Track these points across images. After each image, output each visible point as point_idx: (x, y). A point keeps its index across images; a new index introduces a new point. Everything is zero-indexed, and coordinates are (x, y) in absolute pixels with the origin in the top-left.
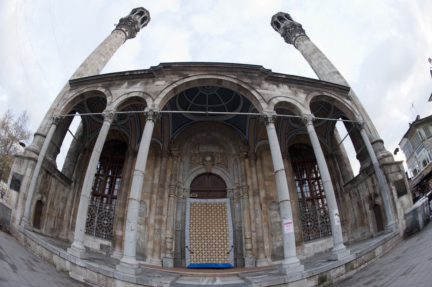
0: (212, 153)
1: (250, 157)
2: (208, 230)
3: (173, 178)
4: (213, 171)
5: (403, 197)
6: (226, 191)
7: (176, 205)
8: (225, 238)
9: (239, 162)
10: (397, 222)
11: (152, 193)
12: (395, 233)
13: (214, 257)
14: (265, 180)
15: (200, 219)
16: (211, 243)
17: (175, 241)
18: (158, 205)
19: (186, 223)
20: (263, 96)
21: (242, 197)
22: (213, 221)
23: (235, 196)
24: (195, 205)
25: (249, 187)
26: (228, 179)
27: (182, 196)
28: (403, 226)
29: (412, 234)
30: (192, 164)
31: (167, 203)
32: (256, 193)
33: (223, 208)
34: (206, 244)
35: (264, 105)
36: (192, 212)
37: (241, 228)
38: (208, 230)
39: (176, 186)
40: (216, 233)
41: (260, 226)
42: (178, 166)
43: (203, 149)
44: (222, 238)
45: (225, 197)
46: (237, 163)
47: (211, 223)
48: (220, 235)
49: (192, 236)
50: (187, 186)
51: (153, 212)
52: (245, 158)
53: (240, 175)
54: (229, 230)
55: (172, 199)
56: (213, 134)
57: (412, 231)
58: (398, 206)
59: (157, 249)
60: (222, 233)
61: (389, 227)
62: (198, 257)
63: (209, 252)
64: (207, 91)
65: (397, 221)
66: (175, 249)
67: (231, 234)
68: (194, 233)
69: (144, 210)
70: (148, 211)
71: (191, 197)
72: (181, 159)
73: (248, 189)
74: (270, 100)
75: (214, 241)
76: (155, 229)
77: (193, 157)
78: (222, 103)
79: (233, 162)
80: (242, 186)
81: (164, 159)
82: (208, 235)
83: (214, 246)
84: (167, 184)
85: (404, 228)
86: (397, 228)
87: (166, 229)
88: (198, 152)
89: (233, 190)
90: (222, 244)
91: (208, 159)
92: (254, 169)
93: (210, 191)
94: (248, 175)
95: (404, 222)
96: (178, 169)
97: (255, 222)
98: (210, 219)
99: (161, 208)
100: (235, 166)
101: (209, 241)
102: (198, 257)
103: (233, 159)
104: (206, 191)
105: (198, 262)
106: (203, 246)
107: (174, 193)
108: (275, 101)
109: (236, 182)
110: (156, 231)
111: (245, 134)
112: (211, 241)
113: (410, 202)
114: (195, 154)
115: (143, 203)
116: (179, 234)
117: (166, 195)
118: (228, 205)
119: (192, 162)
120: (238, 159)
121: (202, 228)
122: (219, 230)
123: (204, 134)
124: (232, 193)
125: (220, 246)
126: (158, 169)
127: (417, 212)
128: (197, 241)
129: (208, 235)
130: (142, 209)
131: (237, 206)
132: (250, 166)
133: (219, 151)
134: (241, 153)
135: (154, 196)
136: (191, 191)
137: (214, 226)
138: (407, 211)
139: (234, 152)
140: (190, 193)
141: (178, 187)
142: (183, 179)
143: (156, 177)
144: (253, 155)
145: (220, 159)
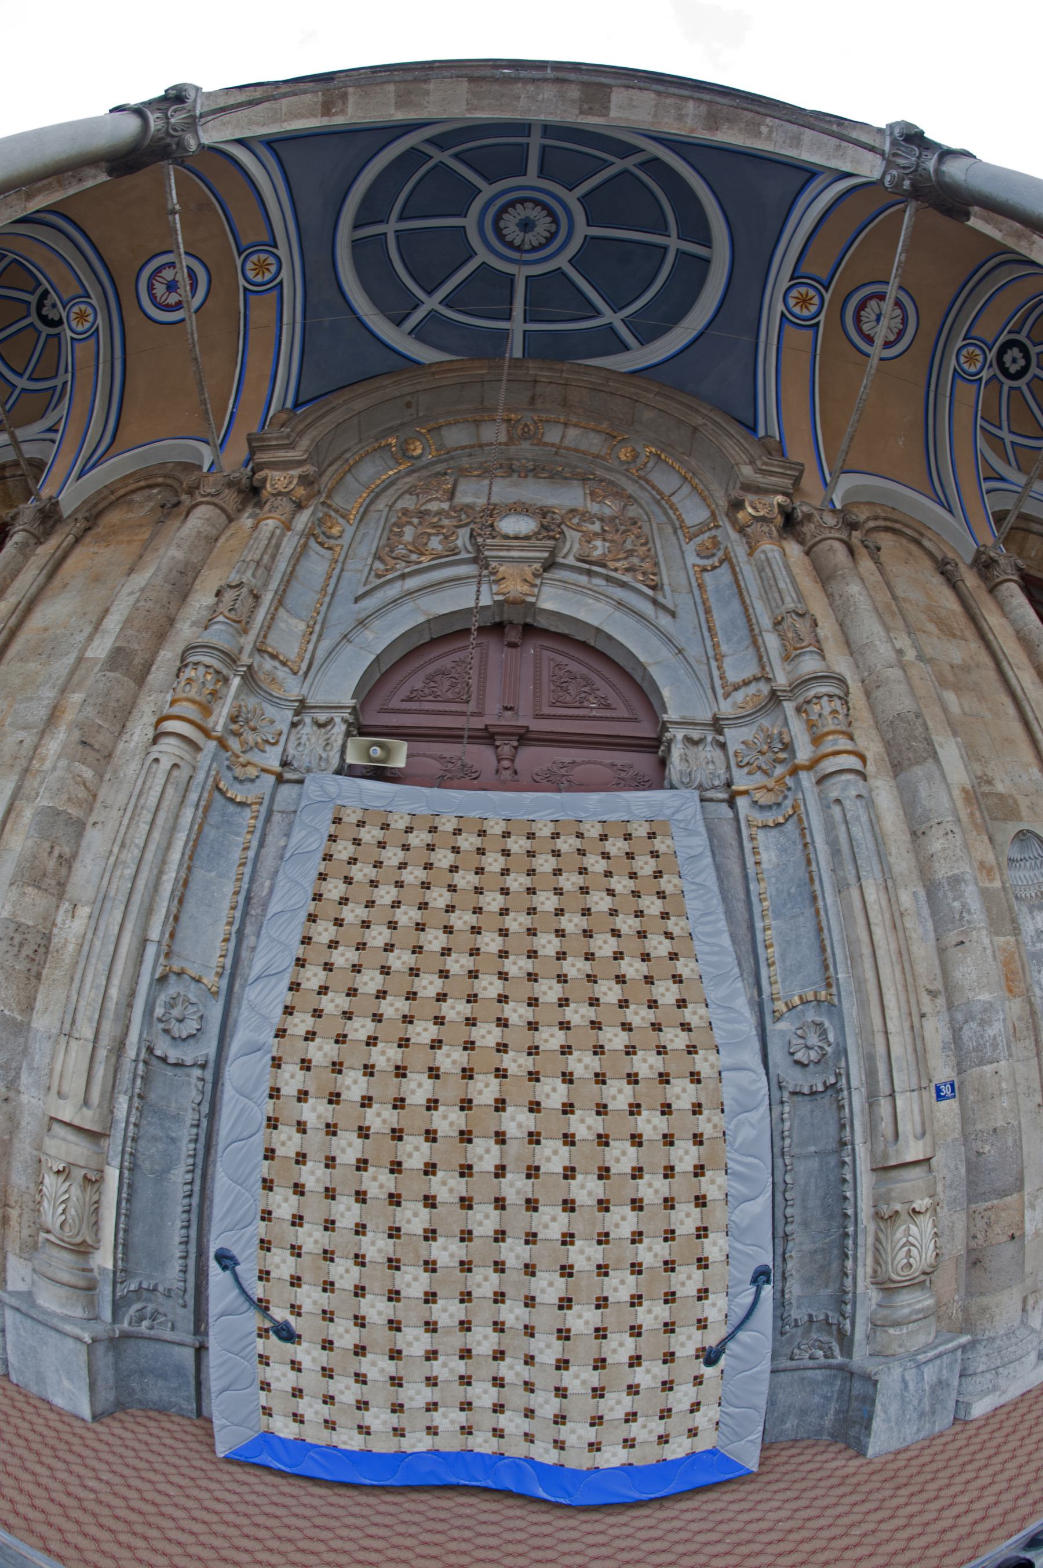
1: (809, 529)
3: (224, 607)
4: (552, 600)
8: (682, 1187)
14: (942, 682)
16: (514, 1252)
17: (131, 1169)
21: (810, 767)
23: (738, 774)
26: (666, 653)
27: (272, 759)
32: (906, 752)
33: (645, 866)
34: (446, 1252)
36: (334, 889)
40: (585, 1125)
44: (652, 1188)
46: (727, 559)
48: (622, 1157)
49: (287, 1142)
50: (339, 686)
53: (765, 621)
54: (728, 1094)
56: (553, 435)
60: (651, 1124)
67: (753, 1127)
68: (315, 1112)
71: (345, 770)
75: (552, 1223)
79: (692, 559)
81: (200, 519)
82: (484, 1155)
84: (168, 655)
89: (717, 725)
93: (524, 737)
96: (282, 566)
101: (484, 1220)
103: (690, 549)
104: (488, 736)
107: (206, 710)
112: (518, 1220)
114: (422, 514)
118: (689, 843)
119: (401, 550)
120: (734, 535)
121: (418, 1059)
123: (493, 433)
125: (621, 1286)
129: (484, 1155)
131: (769, 851)
133: (594, 508)
135: (53, 746)
141: (250, 677)
143: (113, 623)
145: (598, 543)
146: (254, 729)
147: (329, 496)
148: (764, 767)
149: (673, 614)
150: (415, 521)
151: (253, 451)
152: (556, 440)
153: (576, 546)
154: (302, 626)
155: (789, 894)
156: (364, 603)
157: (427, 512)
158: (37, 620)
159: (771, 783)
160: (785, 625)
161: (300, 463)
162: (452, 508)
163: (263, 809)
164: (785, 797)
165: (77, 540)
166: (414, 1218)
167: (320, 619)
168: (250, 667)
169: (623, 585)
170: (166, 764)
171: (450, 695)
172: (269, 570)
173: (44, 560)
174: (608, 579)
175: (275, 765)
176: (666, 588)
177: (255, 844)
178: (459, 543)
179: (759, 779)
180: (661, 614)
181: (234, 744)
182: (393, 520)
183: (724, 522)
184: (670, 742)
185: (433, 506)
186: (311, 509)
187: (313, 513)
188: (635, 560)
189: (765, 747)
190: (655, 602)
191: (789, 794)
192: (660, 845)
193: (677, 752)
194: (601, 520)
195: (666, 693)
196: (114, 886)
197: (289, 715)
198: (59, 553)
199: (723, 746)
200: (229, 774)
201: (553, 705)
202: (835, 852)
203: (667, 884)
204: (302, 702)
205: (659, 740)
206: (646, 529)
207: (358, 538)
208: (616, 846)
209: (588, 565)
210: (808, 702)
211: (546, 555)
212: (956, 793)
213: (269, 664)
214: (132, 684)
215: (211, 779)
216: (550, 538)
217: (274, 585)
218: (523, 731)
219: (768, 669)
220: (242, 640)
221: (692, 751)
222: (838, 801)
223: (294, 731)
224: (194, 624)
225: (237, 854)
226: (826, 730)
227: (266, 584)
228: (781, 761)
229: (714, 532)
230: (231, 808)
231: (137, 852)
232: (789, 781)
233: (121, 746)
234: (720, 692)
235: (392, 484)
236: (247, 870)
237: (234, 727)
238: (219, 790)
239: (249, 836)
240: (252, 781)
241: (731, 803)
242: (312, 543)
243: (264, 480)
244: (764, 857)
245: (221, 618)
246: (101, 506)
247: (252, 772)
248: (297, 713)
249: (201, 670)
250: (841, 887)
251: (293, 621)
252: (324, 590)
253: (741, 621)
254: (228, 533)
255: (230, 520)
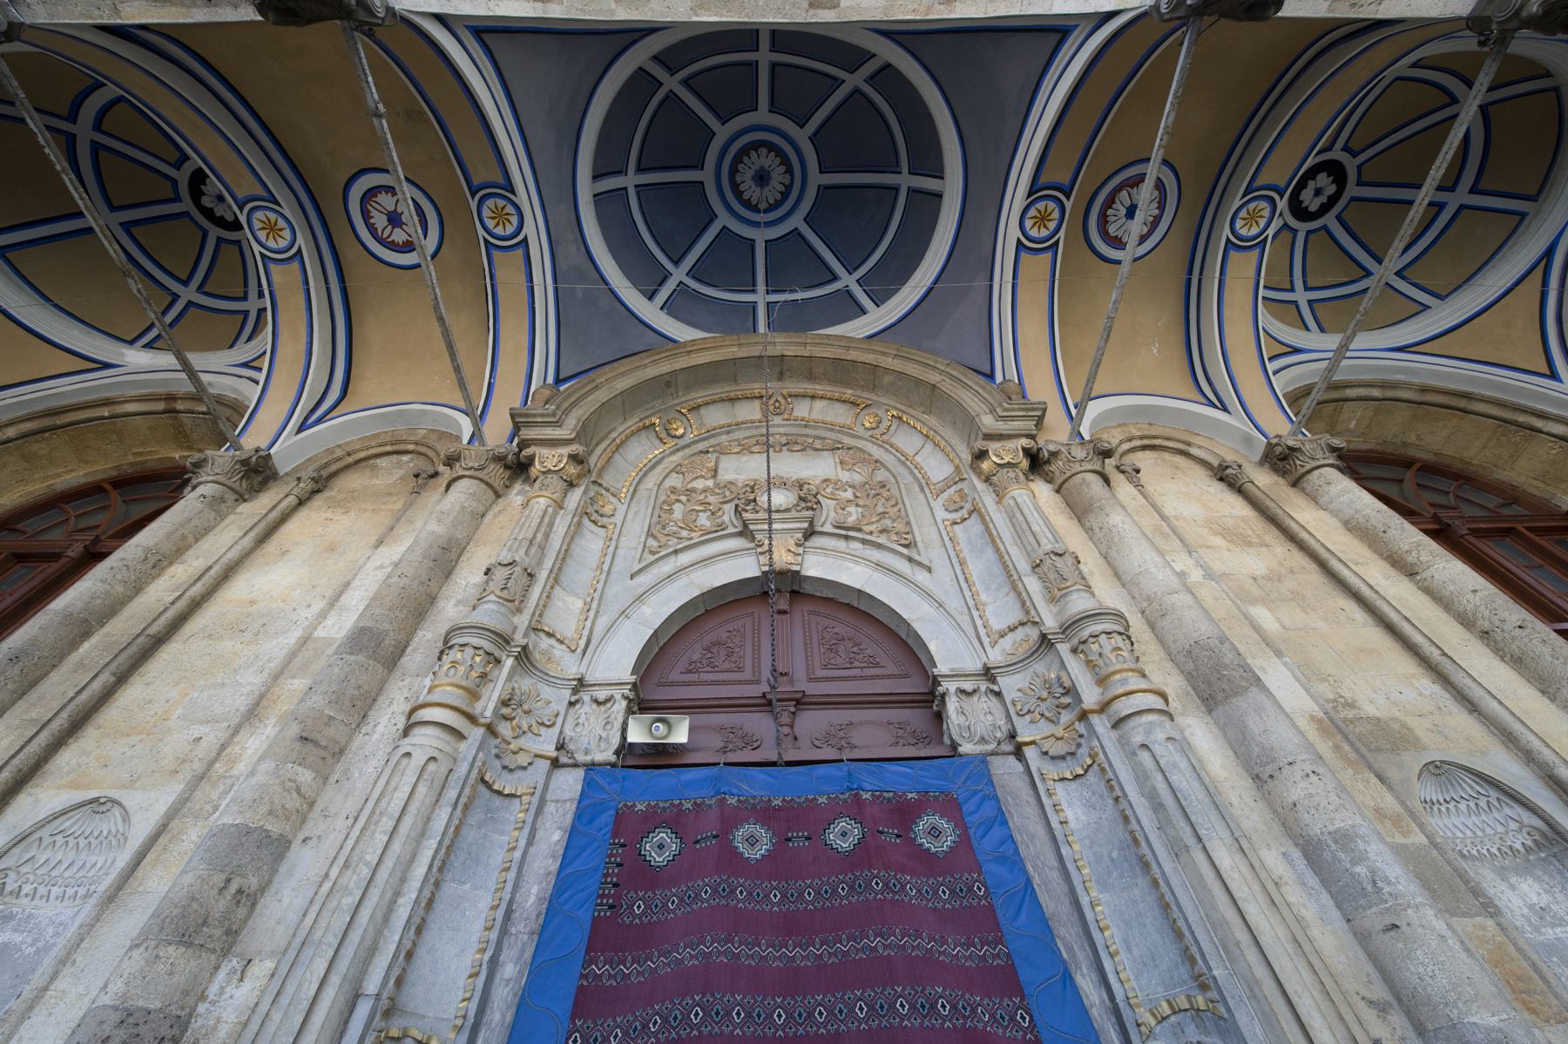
4: (816, 566)
11: (253, 713)
21: (1104, 707)
26: (927, 609)
50: (617, 661)
53: (1023, 565)
56: (802, 409)
77: (678, 508)
79: (941, 514)
80: (1068, 628)
84: (428, 636)
89: (988, 673)
93: (801, 702)
96: (556, 542)
103: (938, 505)
107: (474, 695)
109: (997, 624)
119: (672, 528)
133: (845, 476)
145: (852, 509)
146: (527, 712)
147: (600, 475)
148: (1047, 714)
149: (929, 570)
150: (683, 498)
151: (517, 428)
152: (805, 414)
153: (832, 514)
154: (580, 604)
155: (1112, 859)
156: (639, 579)
157: (693, 490)
158: (239, 589)
159: (1059, 732)
160: (1044, 568)
161: (568, 442)
162: (717, 485)
163: (535, 800)
164: (1079, 745)
165: (301, 503)
167: (597, 596)
168: (525, 648)
169: (879, 546)
170: (419, 758)
171: (726, 666)
172: (542, 548)
173: (250, 522)
174: (864, 542)
176: (919, 544)
177: (523, 842)
178: (726, 518)
179: (1045, 728)
180: (917, 570)
181: (505, 729)
182: (663, 498)
184: (943, 696)
185: (699, 484)
186: (582, 488)
187: (585, 492)
188: (887, 523)
189: (1045, 694)
190: (910, 559)
191: (1082, 741)
193: (952, 705)
194: (852, 487)
195: (932, 647)
196: (323, 924)
197: (566, 694)
198: (274, 514)
199: (998, 694)
200: (497, 763)
201: (825, 667)
202: (1158, 807)
204: (580, 680)
205: (932, 693)
206: (895, 492)
207: (630, 516)
209: (845, 532)
210: (1084, 642)
211: (806, 525)
213: (545, 642)
214: (380, 669)
215: (475, 771)
216: (808, 509)
217: (548, 564)
218: (799, 696)
219: (1033, 613)
220: (515, 620)
221: (968, 703)
222: (1144, 746)
223: (572, 711)
224: (459, 602)
225: (499, 857)
226: (1111, 669)
227: (540, 563)
228: (1066, 707)
229: (959, 486)
230: (498, 801)
231: (366, 872)
232: (1081, 727)
233: (358, 740)
234: (986, 640)
235: (659, 462)
236: (512, 875)
237: (504, 711)
238: (483, 781)
239: (516, 833)
240: (524, 768)
241: (1018, 752)
242: (586, 521)
243: (531, 459)
244: (1069, 814)
245: (492, 597)
246: (334, 468)
247: (523, 759)
248: (575, 691)
249: (469, 651)
250: (1178, 851)
251: (570, 599)
252: (600, 567)
253: (997, 570)
254: (496, 509)
255: (498, 495)
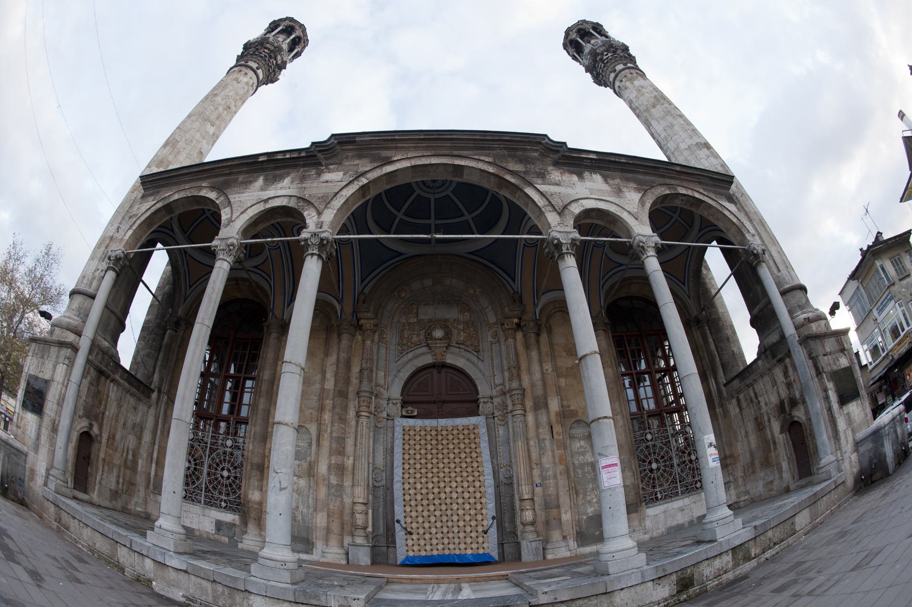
0: (446, 320)
1: (525, 328)
2: (442, 485)
5: (850, 405)
6: (476, 401)
7: (372, 434)
9: (502, 340)
10: (839, 458)
11: (321, 409)
12: (835, 482)
13: (456, 540)
15: (423, 461)
16: (449, 512)
17: (373, 510)
18: (335, 435)
19: (395, 471)
20: (549, 198)
21: (511, 412)
22: (452, 465)
24: (412, 433)
25: (524, 390)
26: (480, 375)
28: (851, 466)
29: (873, 482)
30: (404, 346)
31: (353, 430)
32: (541, 404)
33: (472, 436)
35: (552, 218)
36: (407, 447)
37: (511, 477)
38: (442, 485)
39: (372, 393)
40: (460, 490)
41: (550, 473)
42: (375, 351)
43: (427, 313)
44: (472, 501)
45: (475, 413)
46: (499, 341)
47: (446, 470)
48: (466, 495)
49: (407, 497)
50: (396, 391)
51: (325, 451)
52: (516, 330)
53: (506, 367)
54: (486, 484)
55: (363, 420)
56: (447, 282)
57: (871, 475)
58: (842, 424)
59: (335, 526)
60: (471, 489)
61: (824, 470)
62: (422, 542)
63: (445, 530)
64: (432, 191)
65: (839, 455)
66: (373, 526)
67: (490, 491)
68: (412, 492)
69: (306, 445)
70: (314, 447)
71: (403, 416)
72: (380, 335)
73: (524, 395)
74: (565, 207)
75: (455, 507)
76: (329, 486)
77: (406, 332)
78: (463, 215)
79: (490, 339)
80: (510, 391)
82: (443, 496)
83: (455, 518)
84: (352, 390)
85: (855, 470)
86: (840, 470)
87: (353, 486)
88: (415, 320)
89: (491, 398)
90: (473, 512)
91: (438, 333)
92: (534, 354)
93: (444, 402)
94: (524, 366)
95: (854, 457)
96: (375, 357)
97: (539, 464)
98: (446, 461)
99: (341, 441)
100: (495, 348)
101: (444, 507)
102: (422, 542)
103: (489, 333)
104: (435, 402)
105: (423, 553)
106: (433, 519)
107: (369, 407)
108: (576, 209)
109: (497, 382)
110: (333, 490)
111: (514, 281)
112: (449, 507)
113: (866, 415)
114: (409, 324)
115: (304, 430)
116: (382, 494)
117: (352, 413)
118: (483, 431)
119: (405, 341)
120: (501, 333)
122: (466, 484)
123: (428, 282)
124: (490, 405)
125: (468, 518)
126: (332, 359)
127: (882, 437)
128: (420, 508)
129: (443, 496)
130: (301, 444)
131: (501, 431)
132: (527, 347)
133: (461, 318)
134: (507, 320)
135: (327, 416)
136: (404, 404)
137: (453, 475)
138: (860, 435)
139: (492, 319)
140: (402, 407)
141: (376, 396)
142: (385, 378)
143: (330, 375)
144: (532, 324)
145: (462, 334)
156: (399, 363)
166: (432, 508)
175: (385, 416)
183: (499, 326)
192: (476, 431)
203: (477, 441)
208: (466, 432)
212: (553, 415)
243: (362, 325)
250: (514, 441)
